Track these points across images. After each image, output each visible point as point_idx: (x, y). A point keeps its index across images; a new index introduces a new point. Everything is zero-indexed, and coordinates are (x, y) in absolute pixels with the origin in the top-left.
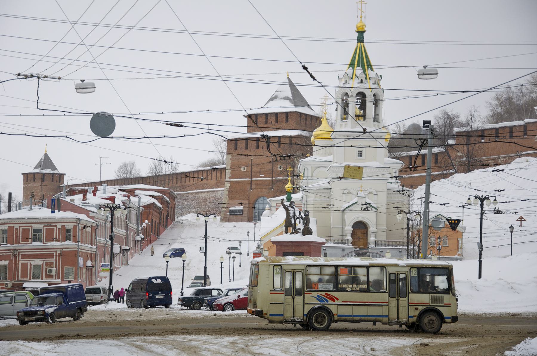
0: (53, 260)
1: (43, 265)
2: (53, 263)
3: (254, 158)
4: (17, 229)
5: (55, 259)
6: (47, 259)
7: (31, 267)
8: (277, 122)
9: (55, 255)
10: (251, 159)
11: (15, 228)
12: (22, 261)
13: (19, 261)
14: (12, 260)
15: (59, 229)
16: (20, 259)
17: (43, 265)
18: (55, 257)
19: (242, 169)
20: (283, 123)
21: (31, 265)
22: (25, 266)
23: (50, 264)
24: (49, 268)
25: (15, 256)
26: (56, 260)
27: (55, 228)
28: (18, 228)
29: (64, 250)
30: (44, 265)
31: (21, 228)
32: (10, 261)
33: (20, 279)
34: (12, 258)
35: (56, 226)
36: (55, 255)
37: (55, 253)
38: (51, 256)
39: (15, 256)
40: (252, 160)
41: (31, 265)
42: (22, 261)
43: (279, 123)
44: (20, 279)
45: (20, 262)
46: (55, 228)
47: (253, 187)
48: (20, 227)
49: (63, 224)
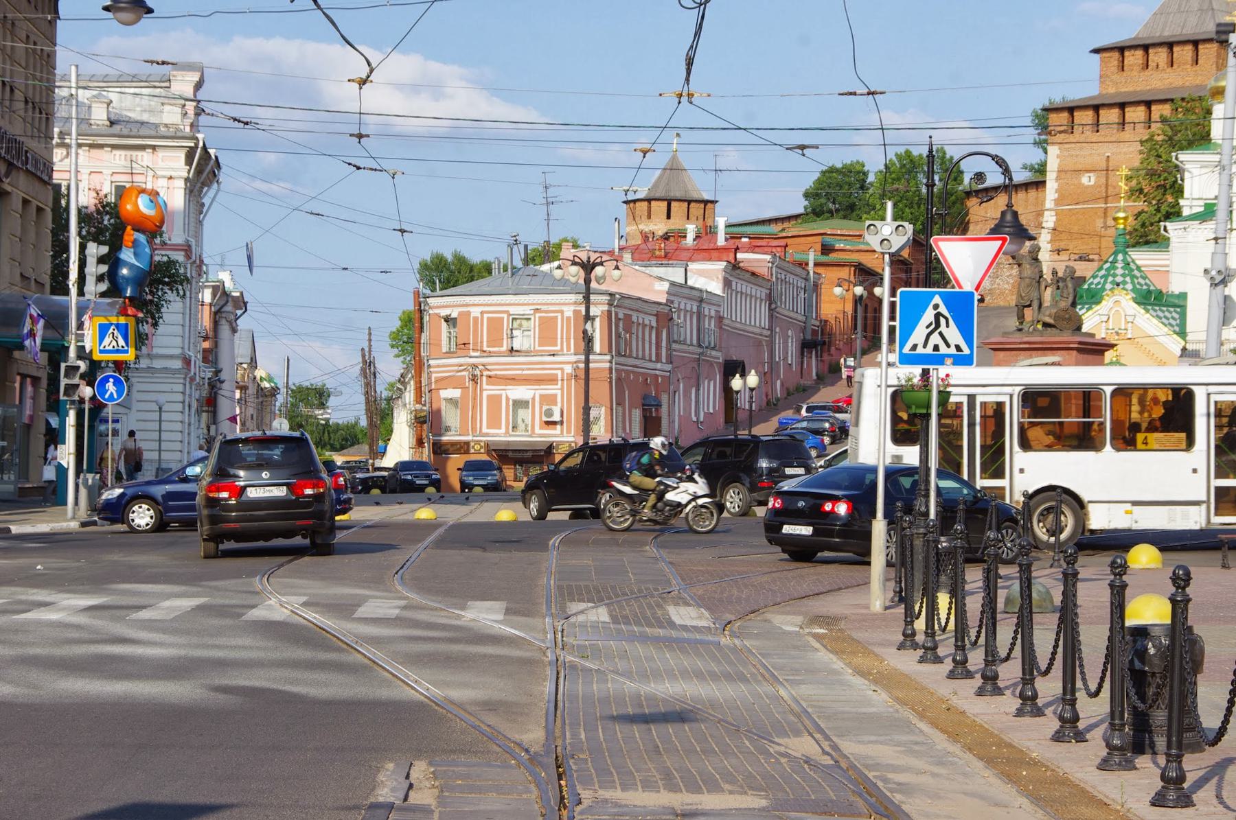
0: (553, 389)
1: (533, 399)
2: (555, 396)
3: (1113, 154)
4: (476, 319)
5: (559, 386)
6: (542, 387)
9: (560, 377)
10: (1107, 154)
12: (488, 390)
14: (468, 388)
15: (569, 318)
16: (485, 386)
17: (533, 399)
18: (560, 382)
20: (1185, 67)
21: (507, 399)
22: (495, 401)
23: (550, 399)
25: (474, 379)
26: (562, 389)
30: (537, 399)
31: (486, 316)
33: (485, 430)
34: (467, 384)
35: (562, 312)
36: (560, 377)
37: (559, 372)
38: (552, 380)
39: (474, 379)
40: (1108, 157)
41: (507, 399)
42: (488, 390)
43: (1175, 66)
44: (485, 430)
45: (485, 394)
46: (559, 315)
48: (482, 313)
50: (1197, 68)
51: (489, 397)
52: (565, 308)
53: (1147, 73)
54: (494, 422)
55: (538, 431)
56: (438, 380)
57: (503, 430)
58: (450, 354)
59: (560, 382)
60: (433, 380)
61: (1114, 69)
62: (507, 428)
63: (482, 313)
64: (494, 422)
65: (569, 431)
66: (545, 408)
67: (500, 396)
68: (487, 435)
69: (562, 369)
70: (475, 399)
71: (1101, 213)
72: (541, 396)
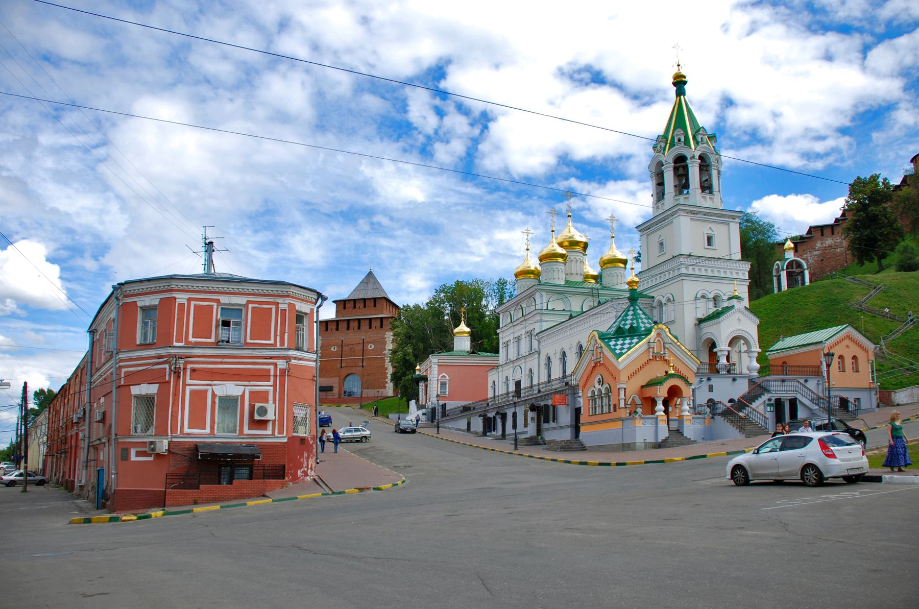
0: (265, 386)
2: (267, 392)
3: (344, 339)
4: (181, 306)
5: (271, 383)
6: (252, 383)
7: (213, 402)
8: (365, 307)
9: (272, 373)
11: (178, 301)
12: (193, 385)
13: (185, 385)
14: (169, 382)
15: (284, 311)
16: (189, 381)
17: (243, 396)
18: (272, 379)
19: (333, 349)
21: (214, 395)
22: (199, 397)
23: (261, 396)
24: (257, 405)
26: (274, 386)
27: (274, 307)
28: (185, 302)
29: (293, 362)
31: (193, 303)
32: (164, 384)
33: (186, 430)
34: (167, 378)
36: (272, 373)
37: (272, 367)
38: (263, 376)
39: (177, 373)
41: (214, 395)
43: (367, 307)
44: (186, 430)
45: (188, 389)
46: (274, 307)
47: (343, 365)
48: (189, 300)
49: (292, 301)
50: (375, 308)
51: (192, 393)
52: (279, 300)
53: (355, 310)
54: (197, 420)
55: (246, 431)
56: (127, 375)
57: (208, 430)
58: (145, 346)
59: (272, 379)
60: (123, 375)
61: (342, 309)
62: (212, 428)
63: (189, 300)
64: (197, 420)
65: (281, 432)
66: (257, 405)
67: (206, 392)
68: (189, 435)
69: (275, 365)
70: (176, 394)
71: (340, 362)
72: (251, 393)
